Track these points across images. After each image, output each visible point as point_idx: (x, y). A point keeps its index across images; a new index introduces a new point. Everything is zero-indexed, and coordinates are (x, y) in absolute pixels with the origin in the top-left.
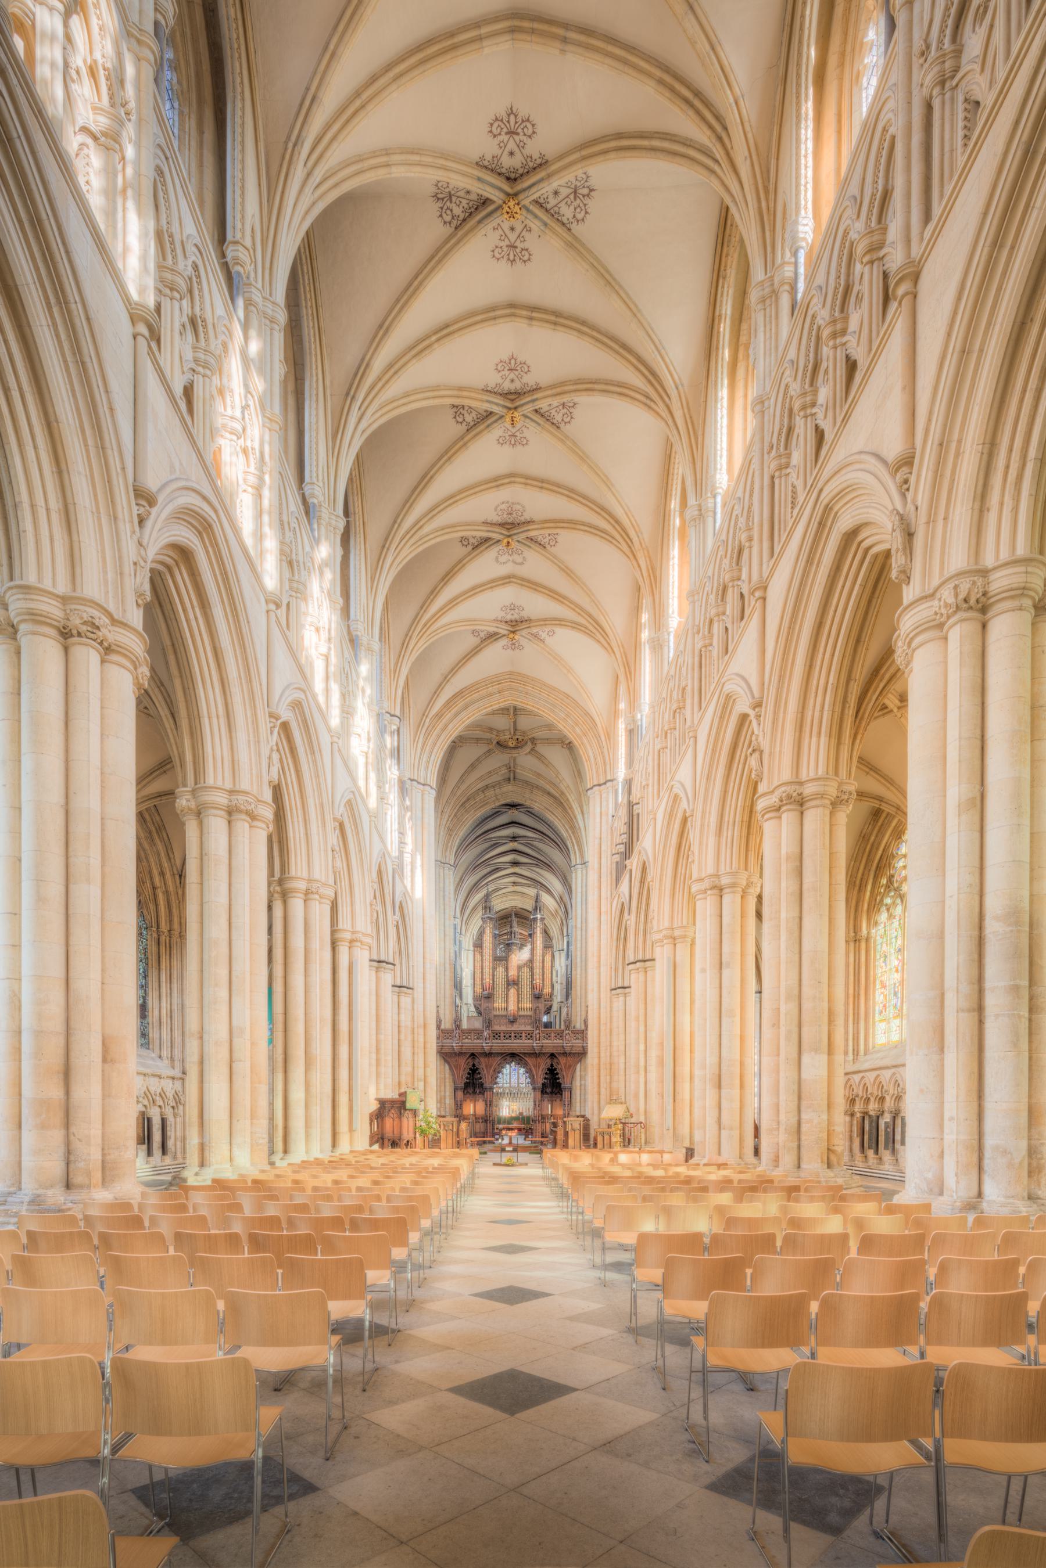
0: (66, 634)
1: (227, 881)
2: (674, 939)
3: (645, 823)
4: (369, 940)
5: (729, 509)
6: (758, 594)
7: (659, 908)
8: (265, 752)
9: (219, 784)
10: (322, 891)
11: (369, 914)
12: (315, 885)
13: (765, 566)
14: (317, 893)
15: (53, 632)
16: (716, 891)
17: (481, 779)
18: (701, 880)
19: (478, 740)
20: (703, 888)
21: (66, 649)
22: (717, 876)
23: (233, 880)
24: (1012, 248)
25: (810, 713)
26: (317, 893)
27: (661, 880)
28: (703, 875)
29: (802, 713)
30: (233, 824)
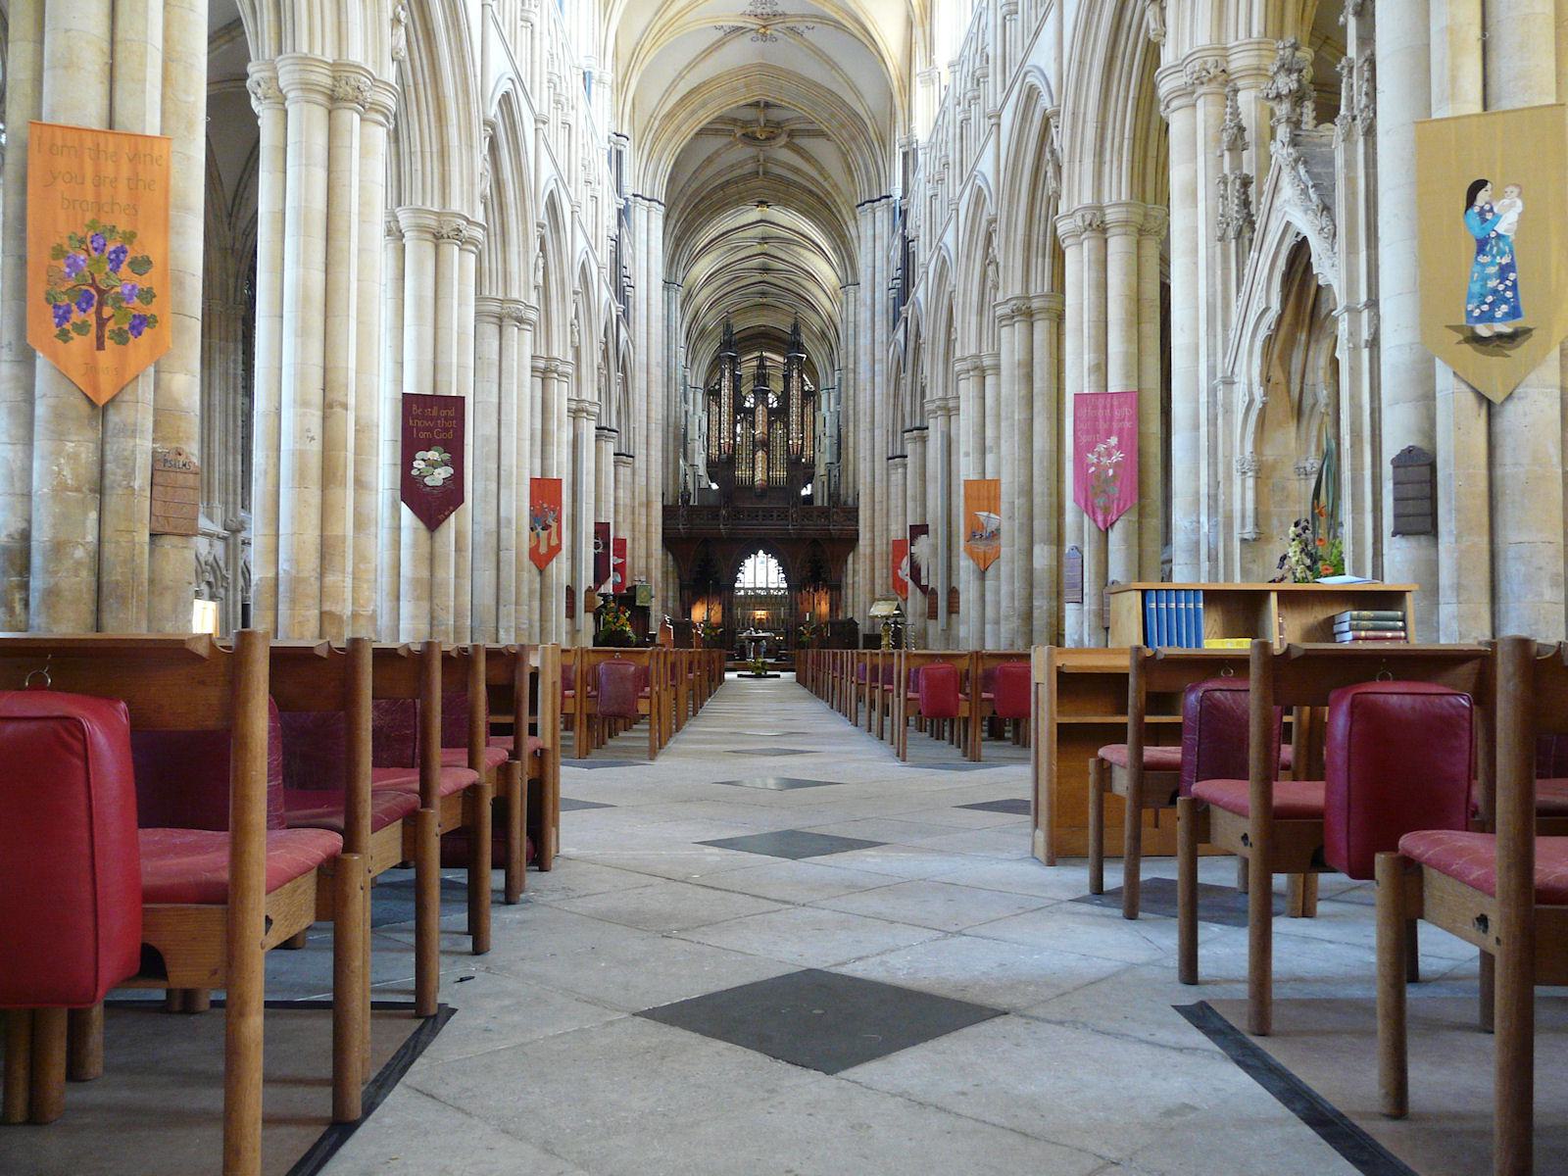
0: (438, 238)
1: (497, 380)
2: (949, 410)
3: (920, 271)
4: (596, 409)
5: (978, 15)
6: (993, 121)
7: (932, 374)
8: (532, 262)
9: (494, 295)
10: (560, 369)
11: (596, 379)
12: (554, 363)
13: (998, 96)
14: (555, 371)
15: (429, 237)
16: (976, 372)
17: (719, 174)
18: (964, 359)
19: (717, 132)
20: (965, 367)
21: (437, 247)
22: (978, 356)
23: (504, 381)
24: (1100, 15)
25: (1035, 237)
26: (555, 371)
27: (933, 344)
28: (966, 355)
29: (1030, 236)
30: (504, 329)
